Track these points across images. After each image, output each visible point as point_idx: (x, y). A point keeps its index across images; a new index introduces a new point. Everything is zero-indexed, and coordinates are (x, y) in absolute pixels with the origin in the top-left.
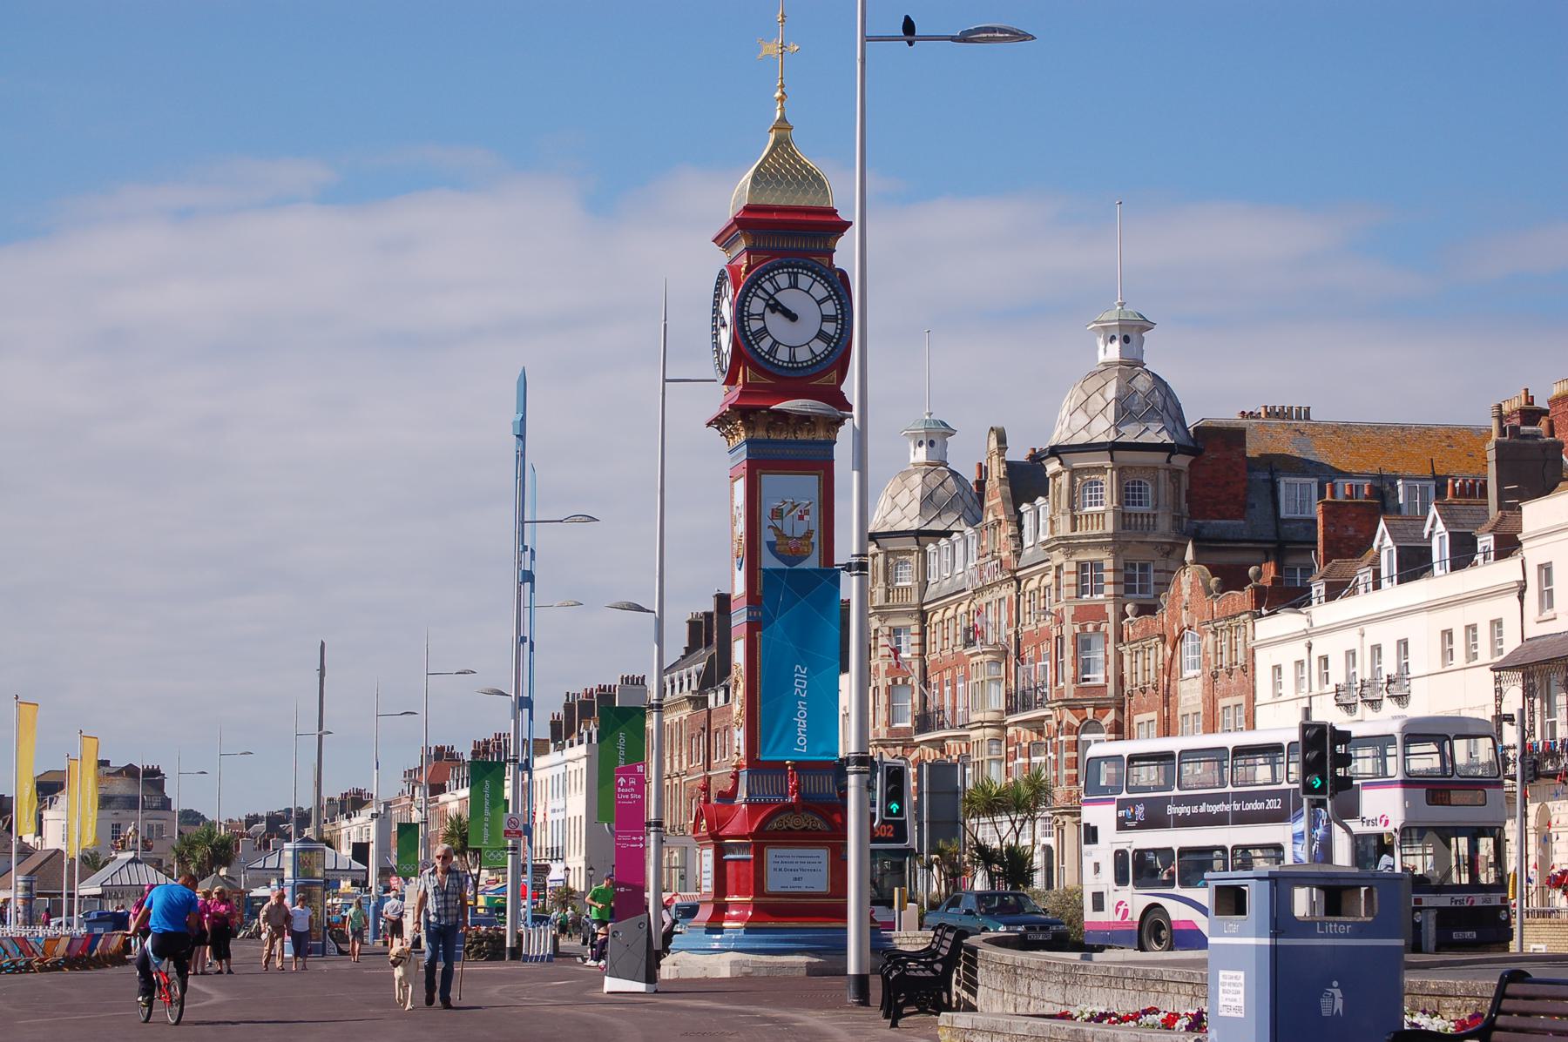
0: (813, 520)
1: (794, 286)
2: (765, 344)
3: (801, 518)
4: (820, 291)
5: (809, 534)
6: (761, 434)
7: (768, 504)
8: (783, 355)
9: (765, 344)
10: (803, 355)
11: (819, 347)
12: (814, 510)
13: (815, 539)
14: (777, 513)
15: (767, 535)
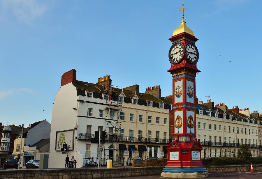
0: (182, 89)
1: (177, 47)
2: (173, 59)
3: (180, 89)
4: (180, 47)
5: (181, 92)
6: (174, 75)
7: (176, 87)
8: (175, 60)
9: (173, 59)
10: (178, 59)
11: (180, 57)
12: (193, 88)
13: (182, 92)
14: (176, 89)
15: (175, 93)
